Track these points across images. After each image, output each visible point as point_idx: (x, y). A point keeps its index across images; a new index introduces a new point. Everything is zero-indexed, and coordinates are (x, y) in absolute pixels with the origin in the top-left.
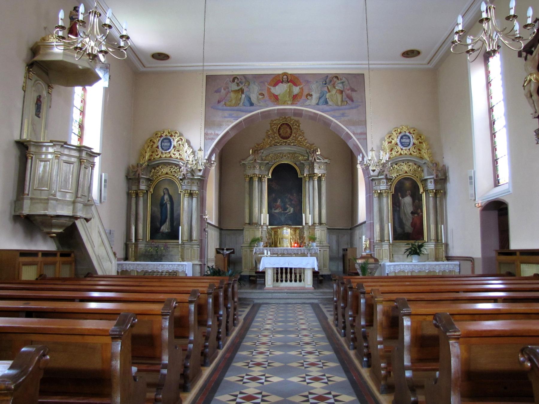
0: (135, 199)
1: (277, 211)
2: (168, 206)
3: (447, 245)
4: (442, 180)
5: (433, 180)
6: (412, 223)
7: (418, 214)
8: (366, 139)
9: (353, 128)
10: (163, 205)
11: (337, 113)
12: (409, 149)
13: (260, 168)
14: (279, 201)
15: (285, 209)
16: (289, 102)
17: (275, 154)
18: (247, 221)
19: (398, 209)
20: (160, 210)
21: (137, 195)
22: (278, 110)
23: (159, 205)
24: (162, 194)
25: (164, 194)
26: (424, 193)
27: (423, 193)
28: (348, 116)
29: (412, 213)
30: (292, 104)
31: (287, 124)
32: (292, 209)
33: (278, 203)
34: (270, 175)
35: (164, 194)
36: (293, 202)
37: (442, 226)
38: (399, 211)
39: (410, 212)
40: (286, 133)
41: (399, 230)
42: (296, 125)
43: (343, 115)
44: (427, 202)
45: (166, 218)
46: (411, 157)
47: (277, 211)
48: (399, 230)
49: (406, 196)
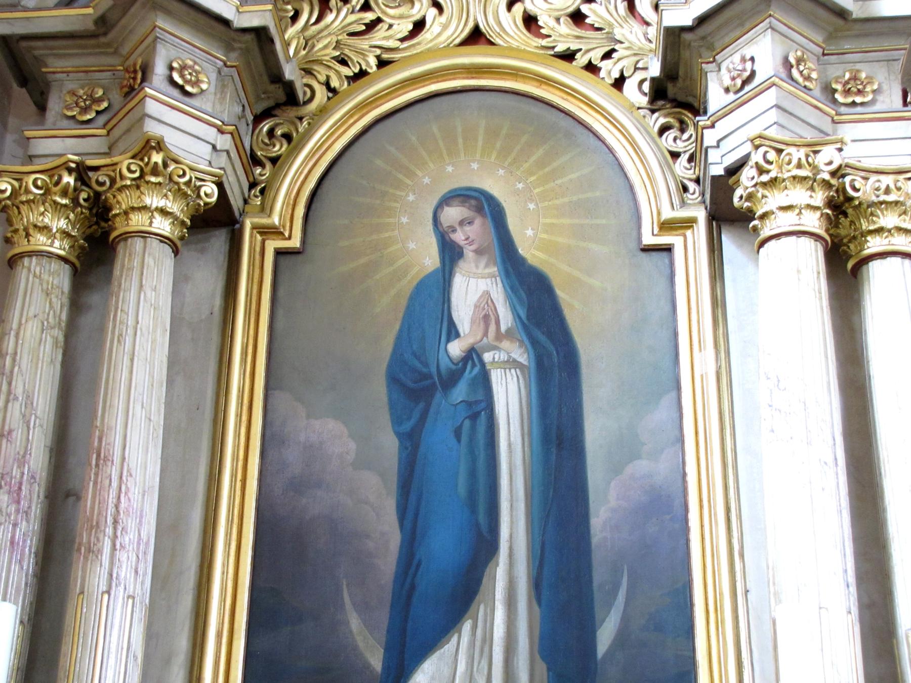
0: (60, 279)
2: (509, 395)
10: (427, 385)
20: (389, 444)
21: (97, 251)
23: (378, 389)
24: (429, 258)
25: (451, 253)
35: (451, 253)
45: (485, 545)
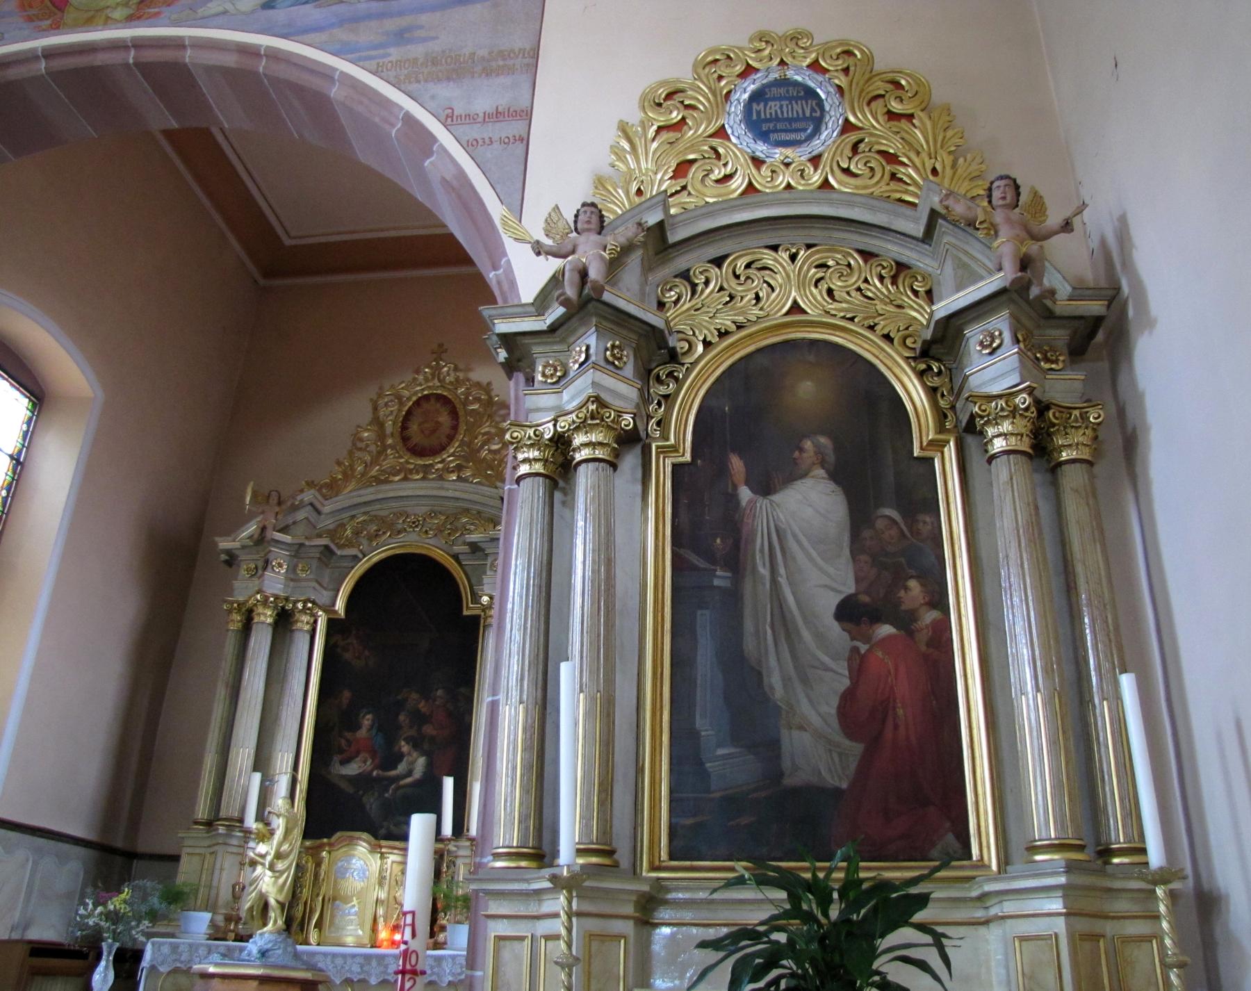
1: (353, 769)
3: (1205, 906)
4: (1088, 333)
5: (1000, 323)
6: (848, 698)
7: (906, 621)
8: (525, 141)
9: (447, 92)
11: (367, 34)
12: (815, 160)
13: (292, 569)
14: (367, 720)
15: (392, 759)
16: (118, 14)
17: (374, 519)
18: (202, 812)
19: (721, 578)
22: (50, 54)
26: (951, 451)
27: (939, 445)
28: (424, 40)
29: (848, 612)
30: (131, 19)
31: (440, 398)
32: (421, 761)
33: (363, 733)
34: (340, 605)
36: (429, 730)
37: (1127, 682)
38: (733, 600)
39: (830, 602)
40: (434, 431)
41: (728, 765)
42: (477, 400)
43: (401, 37)
44: (981, 532)
46: (831, 202)
47: (353, 769)
48: (728, 765)
49: (793, 475)
